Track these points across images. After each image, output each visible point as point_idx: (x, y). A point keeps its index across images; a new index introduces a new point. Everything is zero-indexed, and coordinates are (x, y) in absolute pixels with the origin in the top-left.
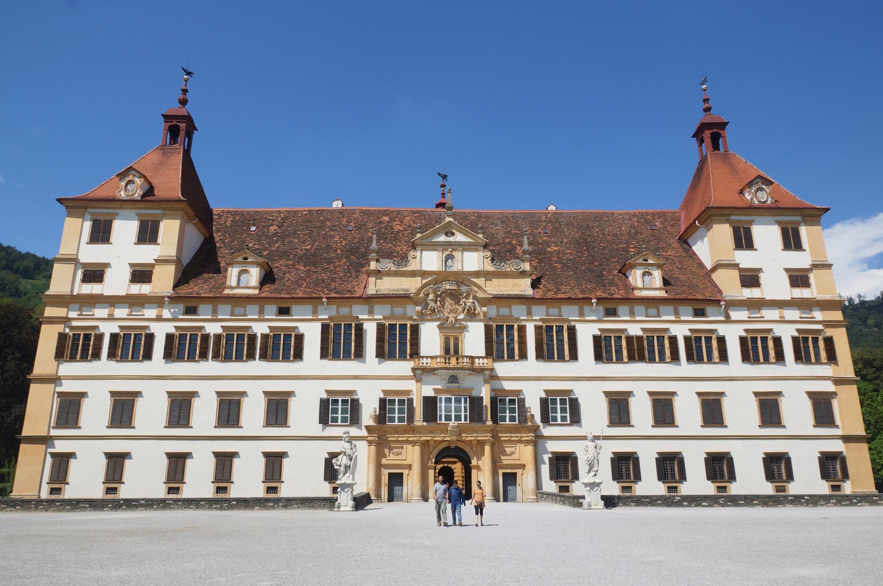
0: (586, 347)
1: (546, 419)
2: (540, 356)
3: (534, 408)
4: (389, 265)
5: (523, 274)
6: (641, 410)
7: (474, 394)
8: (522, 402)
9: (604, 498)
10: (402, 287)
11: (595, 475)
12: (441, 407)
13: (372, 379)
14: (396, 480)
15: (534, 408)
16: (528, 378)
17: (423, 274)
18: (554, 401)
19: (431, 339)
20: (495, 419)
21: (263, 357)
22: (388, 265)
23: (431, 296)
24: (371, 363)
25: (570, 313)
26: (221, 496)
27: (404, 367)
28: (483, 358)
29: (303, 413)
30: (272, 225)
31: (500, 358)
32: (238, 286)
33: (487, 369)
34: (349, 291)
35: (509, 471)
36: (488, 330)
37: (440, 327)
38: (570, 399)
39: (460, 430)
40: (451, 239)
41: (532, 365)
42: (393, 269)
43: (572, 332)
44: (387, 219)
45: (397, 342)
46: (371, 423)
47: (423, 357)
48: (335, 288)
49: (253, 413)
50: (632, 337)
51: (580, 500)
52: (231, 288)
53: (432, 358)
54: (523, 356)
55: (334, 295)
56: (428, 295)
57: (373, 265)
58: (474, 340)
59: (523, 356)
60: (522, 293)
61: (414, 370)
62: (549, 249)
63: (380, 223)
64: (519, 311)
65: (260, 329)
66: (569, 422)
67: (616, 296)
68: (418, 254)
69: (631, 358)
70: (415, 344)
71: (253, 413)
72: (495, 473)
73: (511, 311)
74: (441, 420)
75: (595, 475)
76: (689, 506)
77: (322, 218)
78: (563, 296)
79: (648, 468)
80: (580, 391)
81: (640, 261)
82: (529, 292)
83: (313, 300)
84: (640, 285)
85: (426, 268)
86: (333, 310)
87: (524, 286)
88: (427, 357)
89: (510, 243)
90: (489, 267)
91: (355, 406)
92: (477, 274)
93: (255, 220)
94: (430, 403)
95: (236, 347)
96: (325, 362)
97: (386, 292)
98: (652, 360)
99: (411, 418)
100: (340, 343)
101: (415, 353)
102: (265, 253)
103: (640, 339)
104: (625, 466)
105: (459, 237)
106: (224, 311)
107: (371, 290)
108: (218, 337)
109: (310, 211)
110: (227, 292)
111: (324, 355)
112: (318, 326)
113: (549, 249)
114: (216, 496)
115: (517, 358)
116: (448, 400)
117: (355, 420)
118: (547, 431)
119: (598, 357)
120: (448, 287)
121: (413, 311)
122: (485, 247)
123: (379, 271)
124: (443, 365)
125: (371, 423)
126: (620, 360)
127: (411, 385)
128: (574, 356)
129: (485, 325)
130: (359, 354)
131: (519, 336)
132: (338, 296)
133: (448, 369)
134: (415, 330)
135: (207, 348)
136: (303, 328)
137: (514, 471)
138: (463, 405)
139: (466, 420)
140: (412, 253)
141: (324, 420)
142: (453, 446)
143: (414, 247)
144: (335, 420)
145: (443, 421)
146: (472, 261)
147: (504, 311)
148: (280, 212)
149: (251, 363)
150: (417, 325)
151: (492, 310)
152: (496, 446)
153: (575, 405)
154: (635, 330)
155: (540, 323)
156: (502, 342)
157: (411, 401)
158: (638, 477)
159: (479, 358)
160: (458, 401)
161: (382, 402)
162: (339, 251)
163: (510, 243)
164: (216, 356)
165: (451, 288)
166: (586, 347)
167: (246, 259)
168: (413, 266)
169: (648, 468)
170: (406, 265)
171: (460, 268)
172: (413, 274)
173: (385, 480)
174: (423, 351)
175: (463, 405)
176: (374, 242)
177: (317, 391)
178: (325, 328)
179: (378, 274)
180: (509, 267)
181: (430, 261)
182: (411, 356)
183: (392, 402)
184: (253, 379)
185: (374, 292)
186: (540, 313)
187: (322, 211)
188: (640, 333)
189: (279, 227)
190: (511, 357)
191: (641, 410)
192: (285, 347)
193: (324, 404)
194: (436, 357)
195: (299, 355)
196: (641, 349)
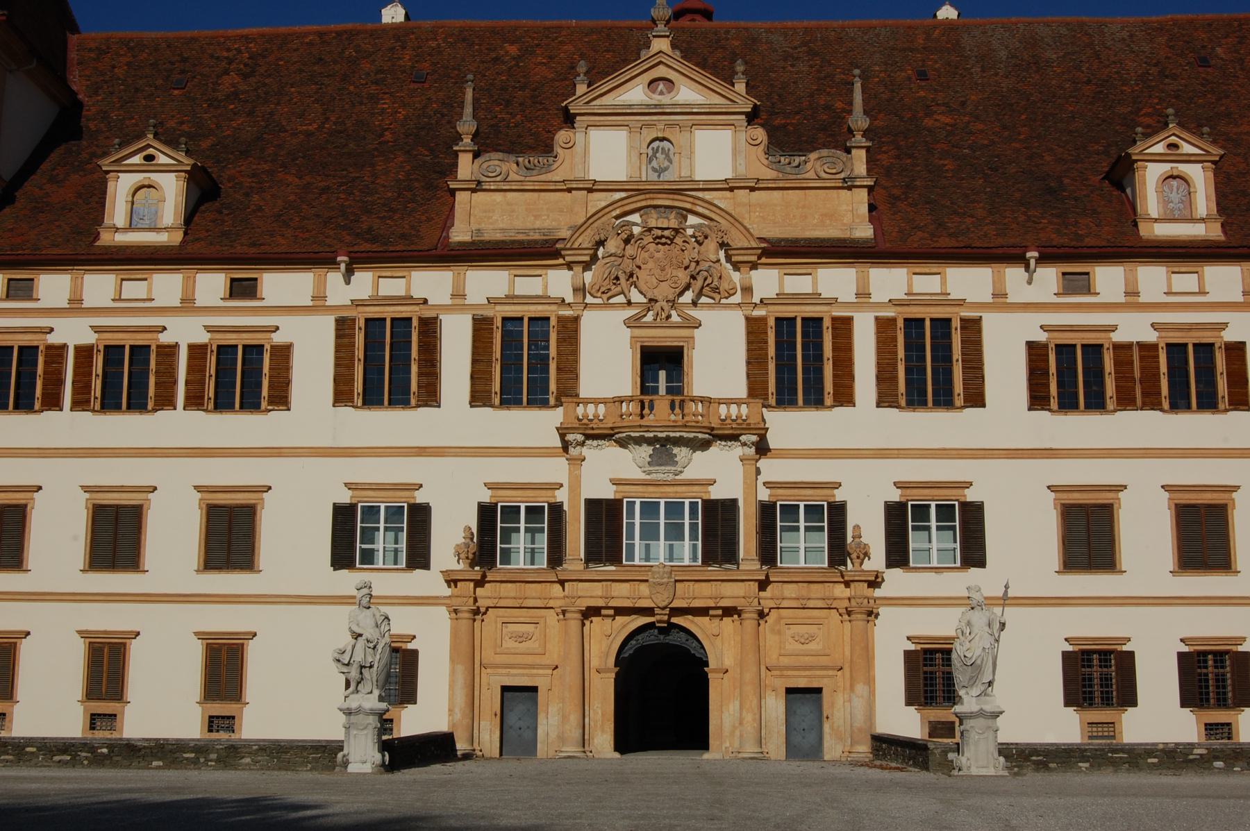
0: (1005, 371)
1: (898, 555)
2: (885, 399)
3: (868, 526)
4: (505, 167)
5: (848, 184)
6: (1146, 534)
7: (716, 493)
8: (838, 511)
9: (1006, 751)
10: (538, 224)
11: (984, 694)
12: (631, 526)
13: (461, 449)
14: (520, 697)
15: (868, 526)
16: (858, 450)
18: (921, 512)
20: (768, 554)
21: (195, 401)
22: (500, 165)
23: (613, 245)
24: (455, 415)
25: (967, 284)
26: (99, 734)
27: (540, 425)
28: (738, 402)
29: (293, 537)
30: (226, 72)
31: (786, 399)
32: (130, 228)
33: (749, 429)
34: (403, 236)
35: (802, 683)
36: (754, 328)
37: (629, 323)
38: (965, 506)
39: (679, 577)
40: (666, 99)
41: (866, 420)
42: (513, 176)
43: (972, 327)
44: (513, 50)
45: (524, 363)
46: (454, 564)
47: (587, 402)
48: (370, 230)
49: (173, 536)
50: (1128, 347)
51: (951, 756)
52: (117, 230)
53: (604, 401)
54: (845, 397)
55: (367, 246)
56: (601, 243)
57: (466, 167)
58: (719, 363)
59: (845, 397)
60: (846, 235)
61: (562, 432)
62: (928, 122)
63: (496, 60)
64: (835, 283)
65: (185, 332)
66: (958, 564)
67: (1088, 241)
68: (579, 137)
69: (1126, 401)
70: (570, 369)
71: (173, 536)
73: (815, 283)
74: (631, 557)
75: (984, 694)
76: (1228, 769)
77: (350, 52)
78: (953, 243)
79: (1158, 679)
80: (986, 485)
81: (1159, 148)
82: (865, 231)
83: (318, 259)
84: (1154, 214)
85: (599, 172)
86: (364, 283)
87: (850, 215)
88: (596, 402)
89: (828, 107)
90: (761, 169)
91: (420, 517)
92: (729, 187)
93: (185, 60)
94: (605, 519)
95: (127, 377)
96: (346, 411)
97: (499, 236)
98: (1179, 403)
99: (556, 556)
100: (387, 364)
101: (568, 391)
102: (206, 144)
103: (1148, 350)
104: (1098, 676)
105: (687, 94)
106: (99, 286)
107: (460, 234)
108: (84, 353)
109: (321, 34)
110: (106, 238)
111: (342, 396)
112: (325, 327)
113: (928, 122)
114: (89, 735)
115: (828, 400)
116: (650, 509)
117: (419, 557)
118: (897, 582)
119: (1038, 399)
120: (652, 223)
121: (559, 282)
122: (752, 117)
123: (479, 183)
124: (635, 420)
125: (454, 564)
126: (1096, 403)
127: (555, 470)
128: (976, 398)
129: (749, 320)
130: (430, 396)
131: (835, 349)
132: (375, 247)
133: (648, 428)
134: (570, 329)
135: (60, 382)
136: (288, 330)
137: (815, 685)
138: (687, 521)
139: (695, 558)
140: (562, 136)
141: (344, 554)
142: (660, 617)
143: (569, 120)
144: (368, 557)
145: (637, 562)
146: (717, 151)
147: (799, 284)
148: (247, 39)
149: (163, 416)
150: (576, 320)
151: (767, 281)
152: (771, 618)
153: (972, 517)
154: (1134, 329)
155: (889, 313)
156: (798, 361)
158: (1128, 698)
159: (729, 402)
160: (674, 509)
161: (486, 513)
162: (388, 136)
163: (828, 107)
164: (81, 403)
165: (660, 223)
166: (1005, 371)
167: (150, 158)
169: (1158, 679)
170: (547, 169)
171: (685, 173)
173: (491, 700)
174: (587, 388)
175: (687, 521)
176: (468, 110)
177: (331, 485)
178: (344, 327)
179: (478, 187)
180: (815, 163)
181: (605, 152)
182: (559, 404)
183: (511, 513)
184: (174, 457)
185: (467, 238)
186: (891, 283)
187: (352, 34)
188: (1151, 337)
189: (245, 76)
190: (815, 400)
191: (1146, 534)
192: (243, 377)
193: (343, 516)
194: (620, 400)
195: (281, 399)
196: (1151, 377)
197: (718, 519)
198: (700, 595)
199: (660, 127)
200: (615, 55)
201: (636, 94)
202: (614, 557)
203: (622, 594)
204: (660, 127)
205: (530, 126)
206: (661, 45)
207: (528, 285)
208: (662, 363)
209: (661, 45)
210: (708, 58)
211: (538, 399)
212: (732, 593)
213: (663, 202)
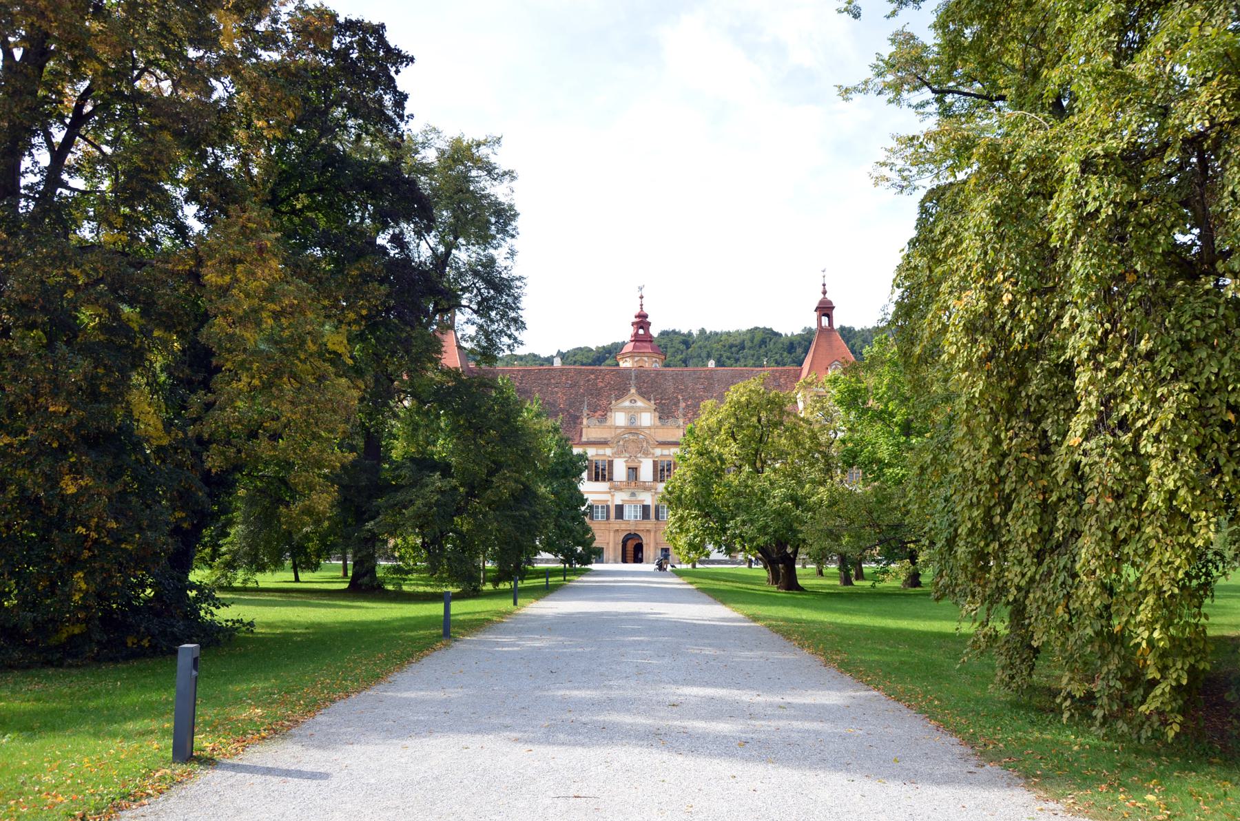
17: (617, 427)
19: (620, 471)
20: (657, 518)
22: (594, 421)
27: (603, 486)
36: (655, 463)
57: (585, 421)
58: (646, 472)
70: (611, 473)
72: (656, 548)
90: (658, 423)
92: (649, 428)
99: (608, 518)
101: (611, 479)
107: (584, 439)
121: (608, 451)
134: (611, 463)
146: (647, 419)
151: (658, 451)
157: (608, 507)
168: (608, 423)
172: (610, 427)
197: (646, 509)
198: (642, 527)
199: (633, 415)
200: (622, 392)
201: (627, 403)
202: (621, 517)
203: (623, 527)
204: (633, 415)
205: (602, 412)
206: (633, 391)
207: (601, 452)
208: (633, 471)
209: (633, 391)
210: (644, 394)
211: (604, 479)
212: (649, 526)
213: (633, 429)
